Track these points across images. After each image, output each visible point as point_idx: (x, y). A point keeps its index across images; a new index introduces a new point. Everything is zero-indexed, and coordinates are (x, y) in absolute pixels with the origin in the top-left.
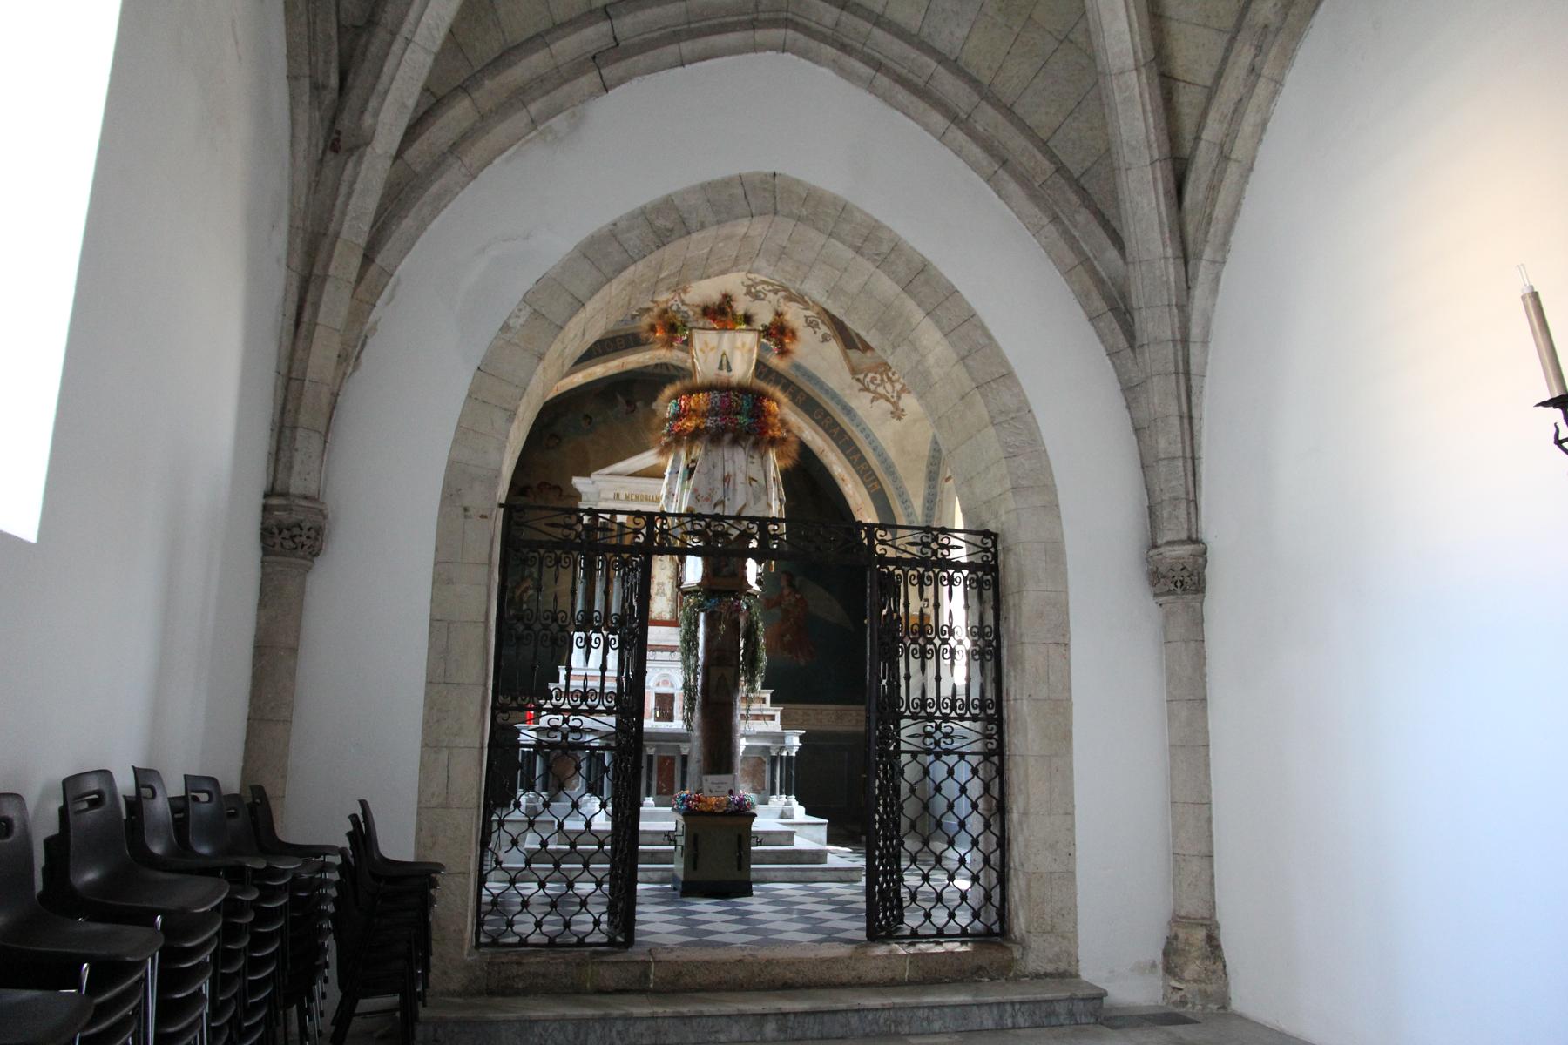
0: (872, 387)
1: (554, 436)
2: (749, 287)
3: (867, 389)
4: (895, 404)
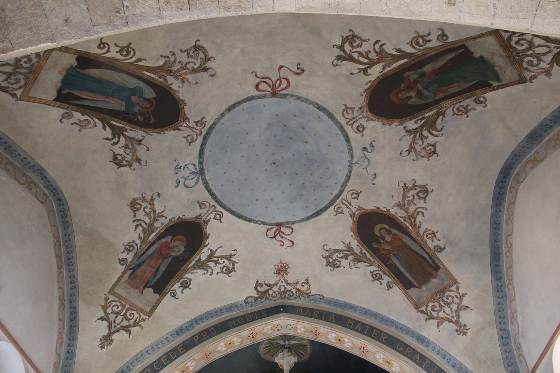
0: (434, 314)
2: (327, 257)
3: (431, 317)
4: (457, 322)
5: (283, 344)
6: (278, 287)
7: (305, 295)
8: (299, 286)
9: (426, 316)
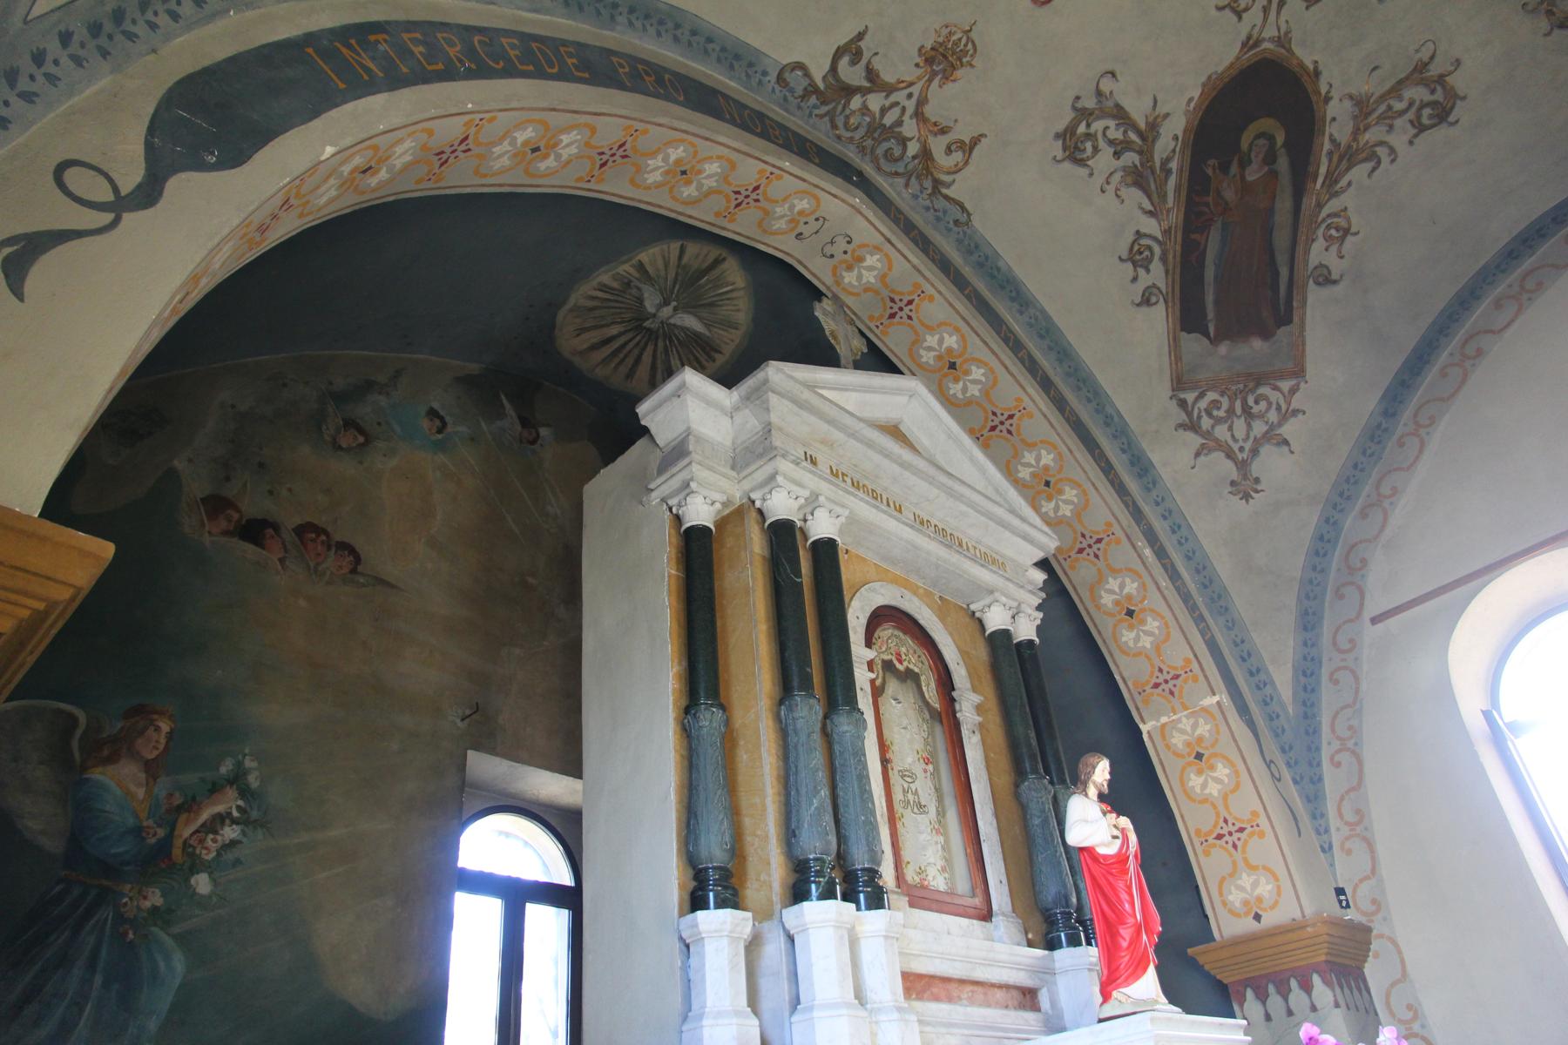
0: (1206, 423)
1: (350, 424)
2: (1083, 114)
3: (1193, 427)
4: (1243, 466)
5: (651, 309)
6: (887, 103)
7: (928, 184)
8: (937, 145)
9: (1183, 417)
